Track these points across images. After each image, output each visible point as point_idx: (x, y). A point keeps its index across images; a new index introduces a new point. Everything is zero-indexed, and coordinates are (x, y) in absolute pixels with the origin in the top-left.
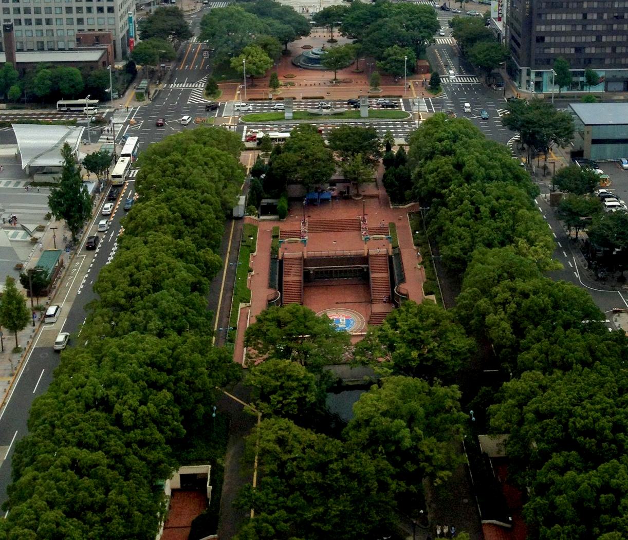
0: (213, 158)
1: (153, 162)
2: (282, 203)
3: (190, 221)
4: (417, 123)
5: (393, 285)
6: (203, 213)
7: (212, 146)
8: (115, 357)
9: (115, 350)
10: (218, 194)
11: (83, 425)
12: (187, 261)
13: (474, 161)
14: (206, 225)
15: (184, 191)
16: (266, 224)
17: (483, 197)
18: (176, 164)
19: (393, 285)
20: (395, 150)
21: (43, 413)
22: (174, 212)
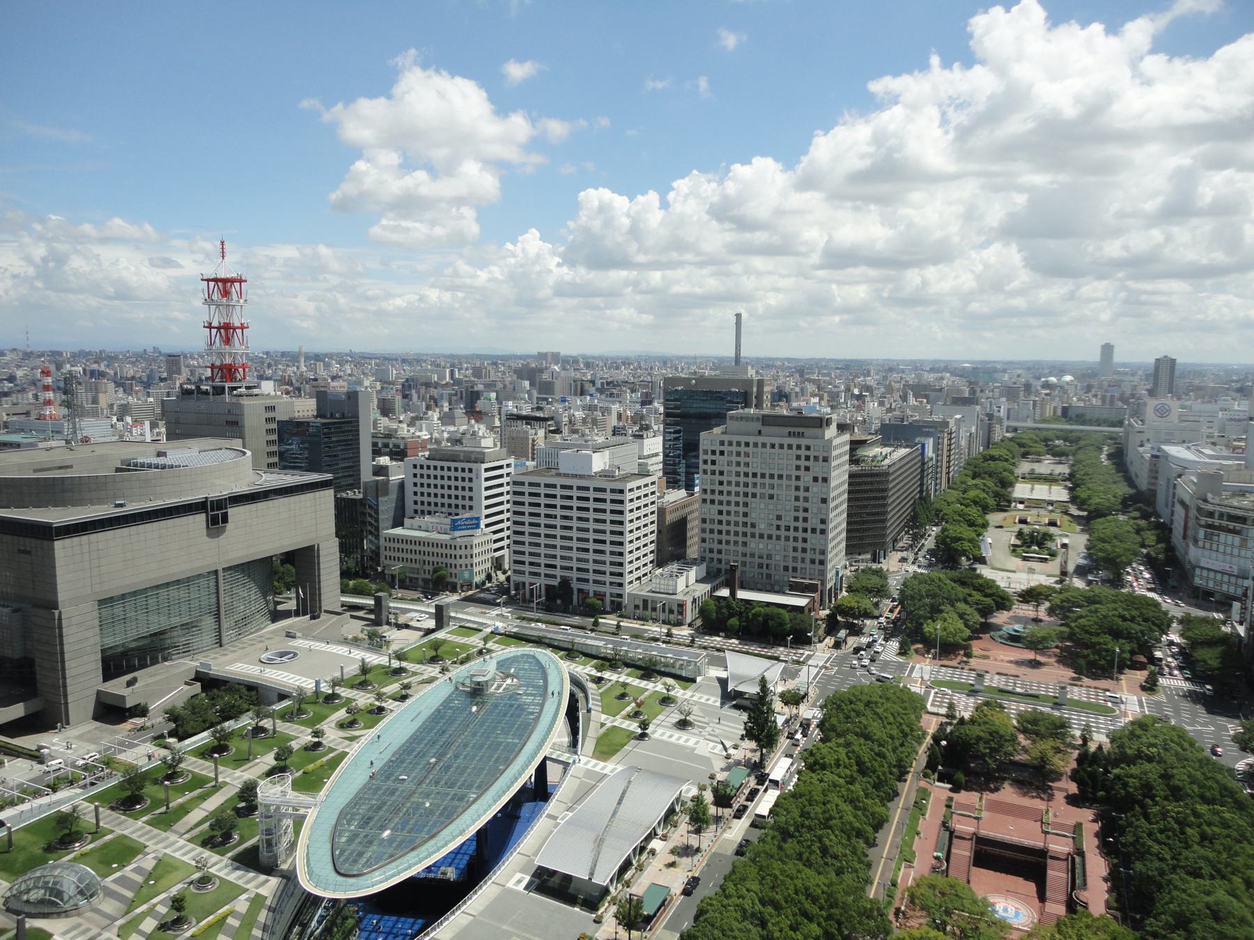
0: (893, 714)
1: (839, 707)
2: (961, 777)
3: (863, 770)
4: (1122, 722)
5: (1073, 888)
6: (876, 764)
7: (894, 703)
8: (776, 877)
9: (777, 873)
10: (894, 750)
11: (736, 933)
12: (856, 808)
13: (1186, 777)
14: (878, 777)
15: (862, 741)
16: (940, 790)
17: (1192, 819)
18: (858, 714)
19: (1073, 888)
20: (1092, 747)
21: (707, 912)
22: (849, 758)
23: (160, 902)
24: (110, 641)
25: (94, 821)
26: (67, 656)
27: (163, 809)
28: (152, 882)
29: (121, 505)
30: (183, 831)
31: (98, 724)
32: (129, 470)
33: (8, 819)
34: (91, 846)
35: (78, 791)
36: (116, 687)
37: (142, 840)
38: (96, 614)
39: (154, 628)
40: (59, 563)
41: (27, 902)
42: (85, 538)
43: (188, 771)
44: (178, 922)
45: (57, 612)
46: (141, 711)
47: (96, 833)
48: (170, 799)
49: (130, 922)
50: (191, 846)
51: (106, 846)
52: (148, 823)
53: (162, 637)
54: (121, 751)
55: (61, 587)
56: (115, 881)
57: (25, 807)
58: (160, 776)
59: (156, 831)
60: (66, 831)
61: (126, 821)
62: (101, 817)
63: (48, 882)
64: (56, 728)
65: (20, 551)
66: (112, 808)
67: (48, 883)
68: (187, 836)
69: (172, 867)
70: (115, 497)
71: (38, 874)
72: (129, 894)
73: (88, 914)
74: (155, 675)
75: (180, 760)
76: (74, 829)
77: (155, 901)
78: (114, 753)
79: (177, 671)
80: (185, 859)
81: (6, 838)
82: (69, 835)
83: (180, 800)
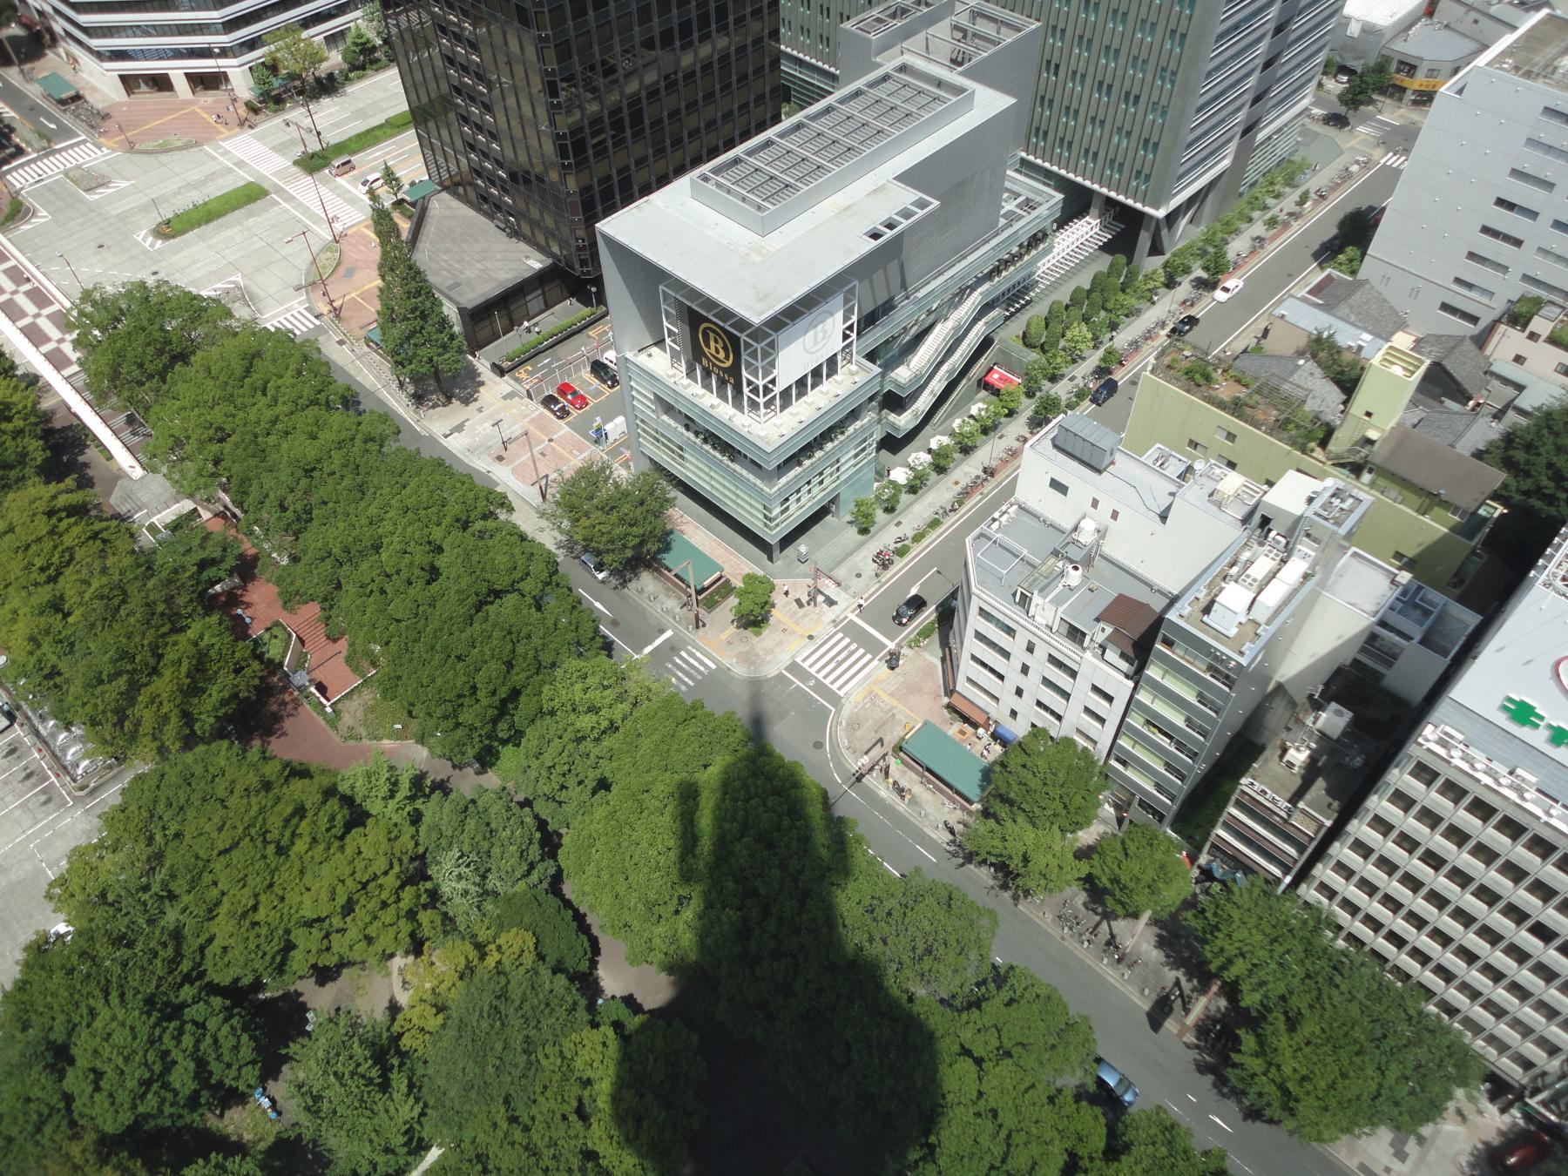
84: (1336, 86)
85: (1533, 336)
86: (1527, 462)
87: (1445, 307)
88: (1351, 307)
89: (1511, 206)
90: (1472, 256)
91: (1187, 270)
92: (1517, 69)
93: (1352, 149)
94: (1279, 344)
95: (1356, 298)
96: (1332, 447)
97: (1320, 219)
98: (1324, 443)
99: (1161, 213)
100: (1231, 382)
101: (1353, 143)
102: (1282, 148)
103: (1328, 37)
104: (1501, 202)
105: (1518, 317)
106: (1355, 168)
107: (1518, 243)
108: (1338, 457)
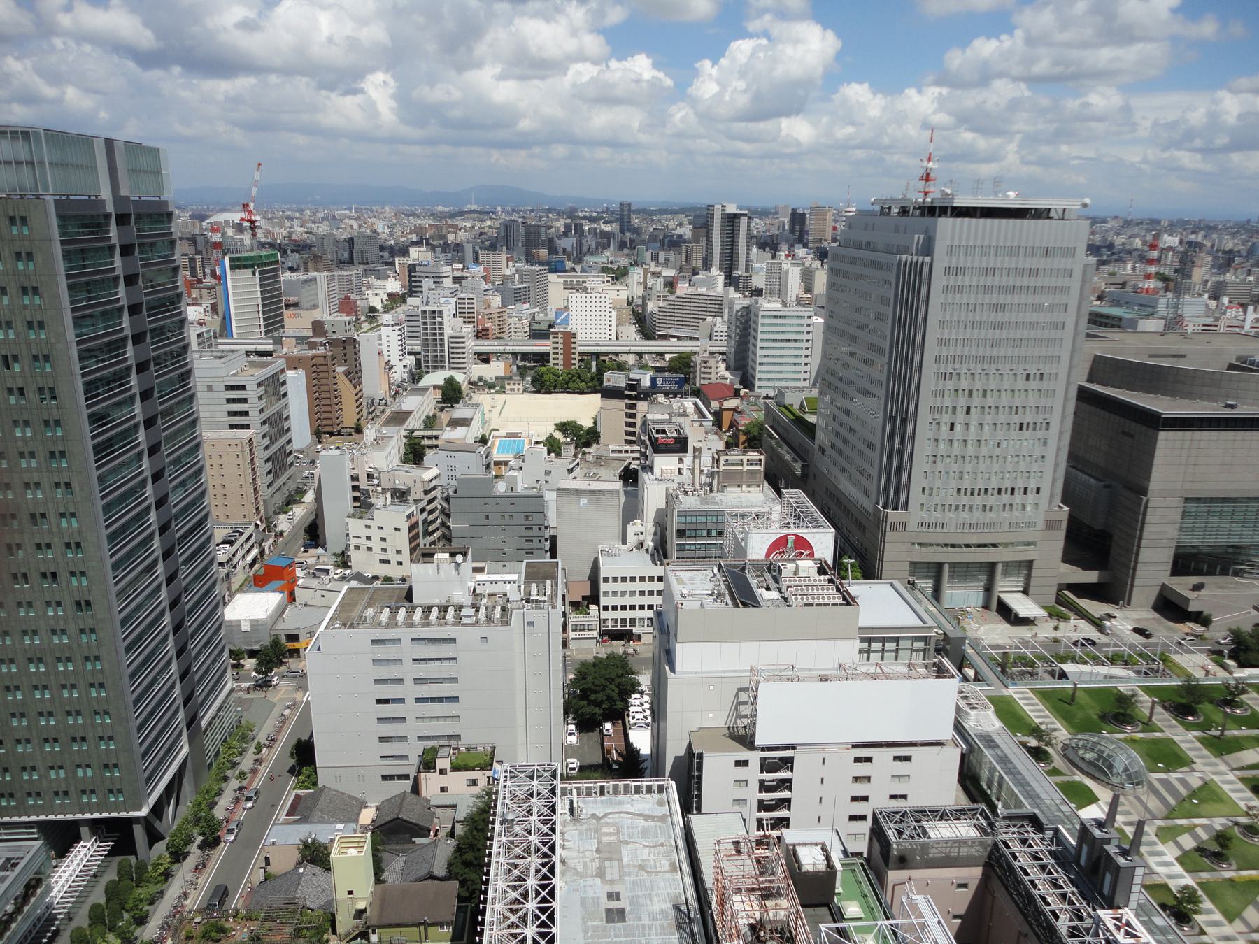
23: (1203, 826)
24: (1187, 540)
25: (1147, 712)
26: (1144, 543)
27: (1217, 733)
28: (1195, 801)
29: (1232, 407)
30: (1234, 766)
31: (1156, 615)
32: (1243, 369)
33: (1071, 672)
34: (1141, 735)
35: (1132, 674)
36: (1182, 585)
37: (1190, 753)
38: (1180, 510)
39: (1235, 539)
40: (1159, 453)
41: (1083, 759)
42: (1188, 434)
43: (1247, 704)
44: (1219, 857)
45: (1145, 499)
46: (1202, 619)
47: (1147, 724)
48: (1227, 726)
49: (1169, 828)
50: (1240, 786)
51: (1155, 742)
52: (1200, 740)
53: (1238, 550)
54: (1177, 652)
55: (1155, 476)
56: (1160, 780)
57: (1086, 668)
58: (1218, 696)
59: (1205, 752)
60: (1122, 711)
61: (1176, 726)
62: (1156, 710)
63: (1103, 752)
64: (1117, 604)
65: (1124, 433)
66: (1165, 708)
67: (1103, 752)
68: (1237, 773)
69: (1218, 796)
70: (1227, 396)
71: (1095, 739)
72: (1172, 802)
73: (1131, 798)
74: (1222, 588)
75: (1244, 692)
76: (1129, 712)
77: (1196, 821)
78: (1170, 651)
79: (1249, 592)
80: (1233, 795)
81: (1070, 692)
82: (1123, 715)
83: (1236, 733)
84: (250, 663)
85: (442, 772)
86: (476, 858)
87: (385, 778)
88: (321, 811)
89: (386, 701)
90: (382, 739)
91: (189, 840)
92: (344, 625)
93: (281, 700)
94: (284, 861)
95: (322, 802)
96: (340, 930)
97: (278, 755)
98: (334, 932)
99: (144, 811)
100: (244, 922)
101: (280, 696)
102: (229, 718)
103: (223, 642)
104: (379, 701)
105: (428, 764)
106: (287, 712)
107: (403, 719)
108: (347, 935)
